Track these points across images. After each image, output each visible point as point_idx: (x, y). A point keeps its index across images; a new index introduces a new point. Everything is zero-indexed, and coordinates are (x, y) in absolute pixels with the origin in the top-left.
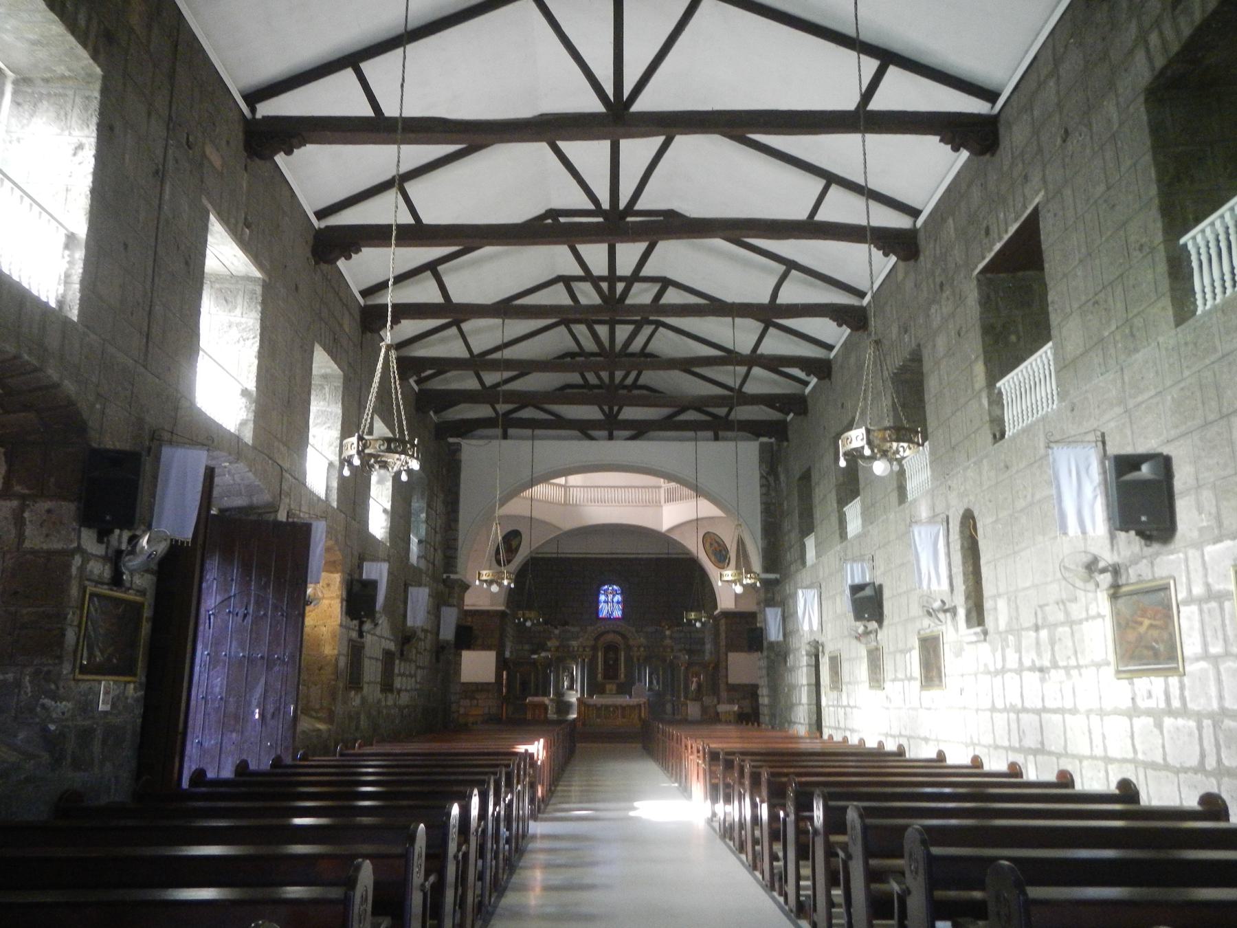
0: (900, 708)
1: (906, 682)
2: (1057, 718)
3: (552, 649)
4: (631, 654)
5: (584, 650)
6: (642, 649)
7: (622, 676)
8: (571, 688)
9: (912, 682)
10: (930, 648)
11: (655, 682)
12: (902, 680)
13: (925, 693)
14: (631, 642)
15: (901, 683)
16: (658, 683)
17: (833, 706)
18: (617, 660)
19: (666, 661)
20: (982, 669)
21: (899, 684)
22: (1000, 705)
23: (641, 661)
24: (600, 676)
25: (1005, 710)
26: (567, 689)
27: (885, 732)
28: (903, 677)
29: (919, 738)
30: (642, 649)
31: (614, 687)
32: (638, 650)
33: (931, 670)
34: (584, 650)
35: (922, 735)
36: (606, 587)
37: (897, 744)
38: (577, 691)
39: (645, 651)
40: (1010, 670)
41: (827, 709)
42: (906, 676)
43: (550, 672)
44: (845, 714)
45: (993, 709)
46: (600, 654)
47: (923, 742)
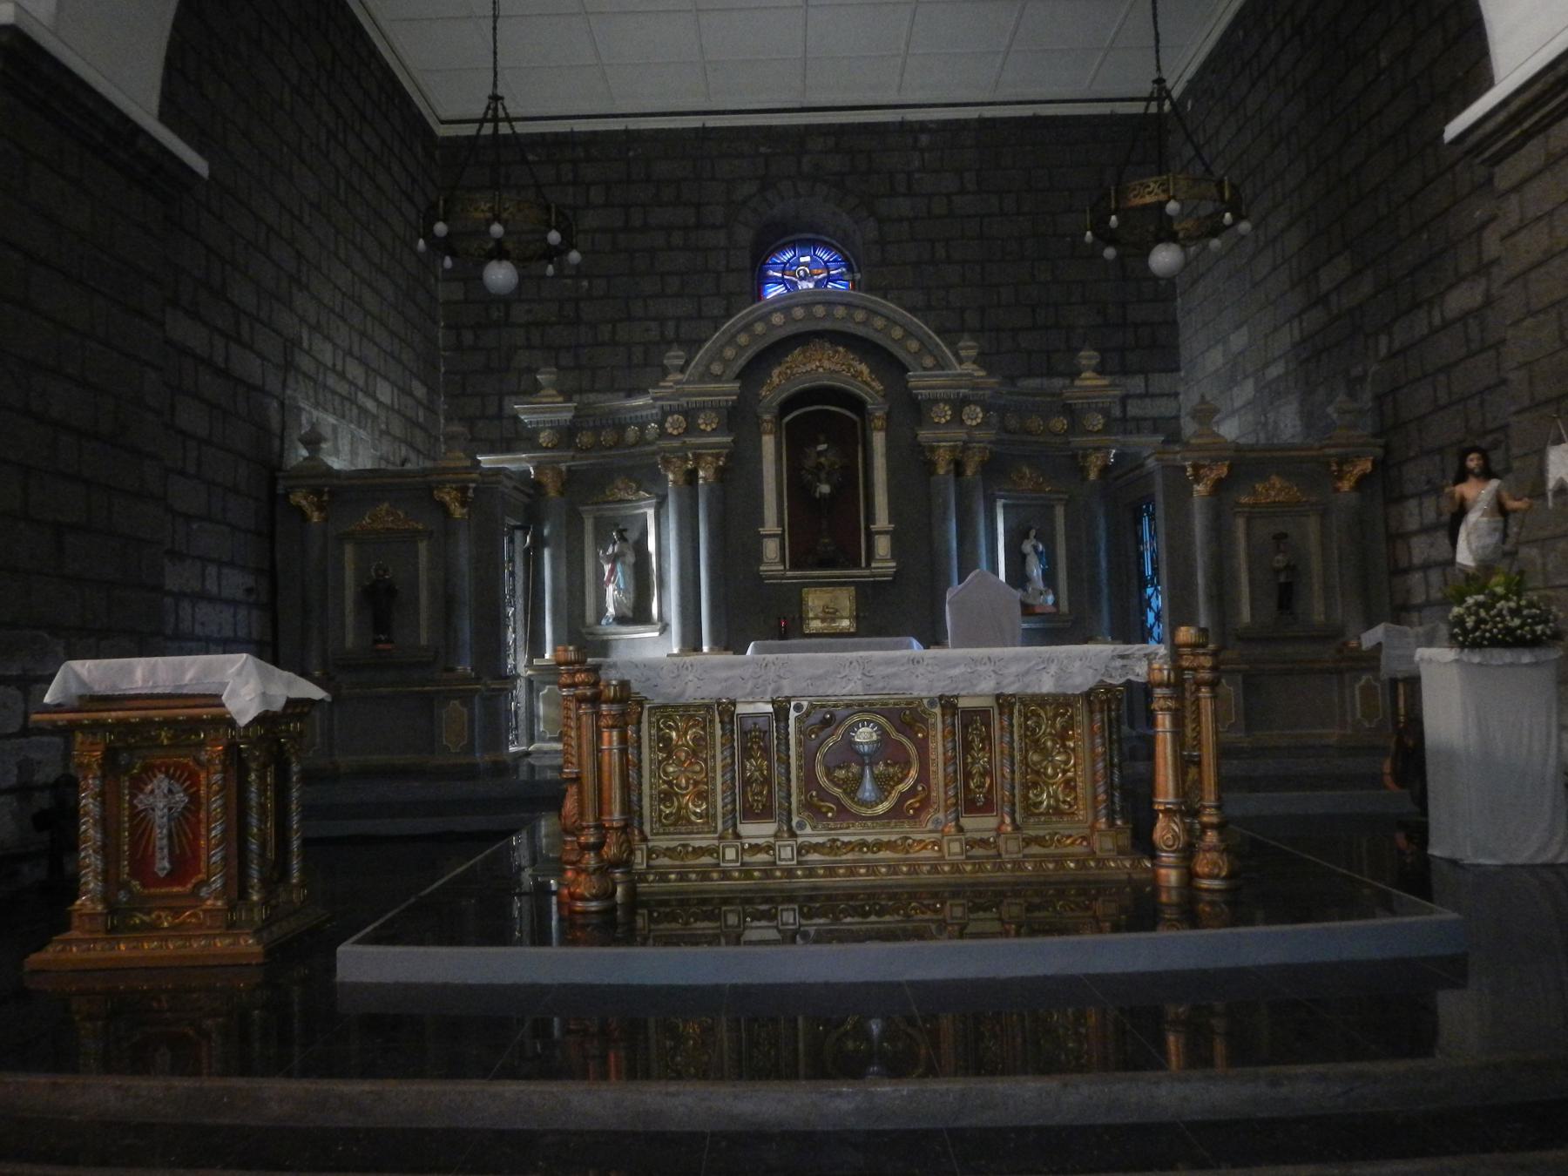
3: (544, 438)
4: (924, 435)
5: (692, 429)
6: (973, 415)
7: (883, 546)
8: (638, 614)
11: (1035, 570)
14: (921, 381)
16: (1049, 578)
18: (852, 484)
19: (1083, 471)
23: (969, 472)
24: (771, 549)
26: (621, 620)
30: (973, 415)
31: (845, 600)
32: (957, 419)
34: (692, 429)
36: (789, 255)
38: (665, 628)
39: (985, 424)
43: (539, 543)
46: (768, 443)
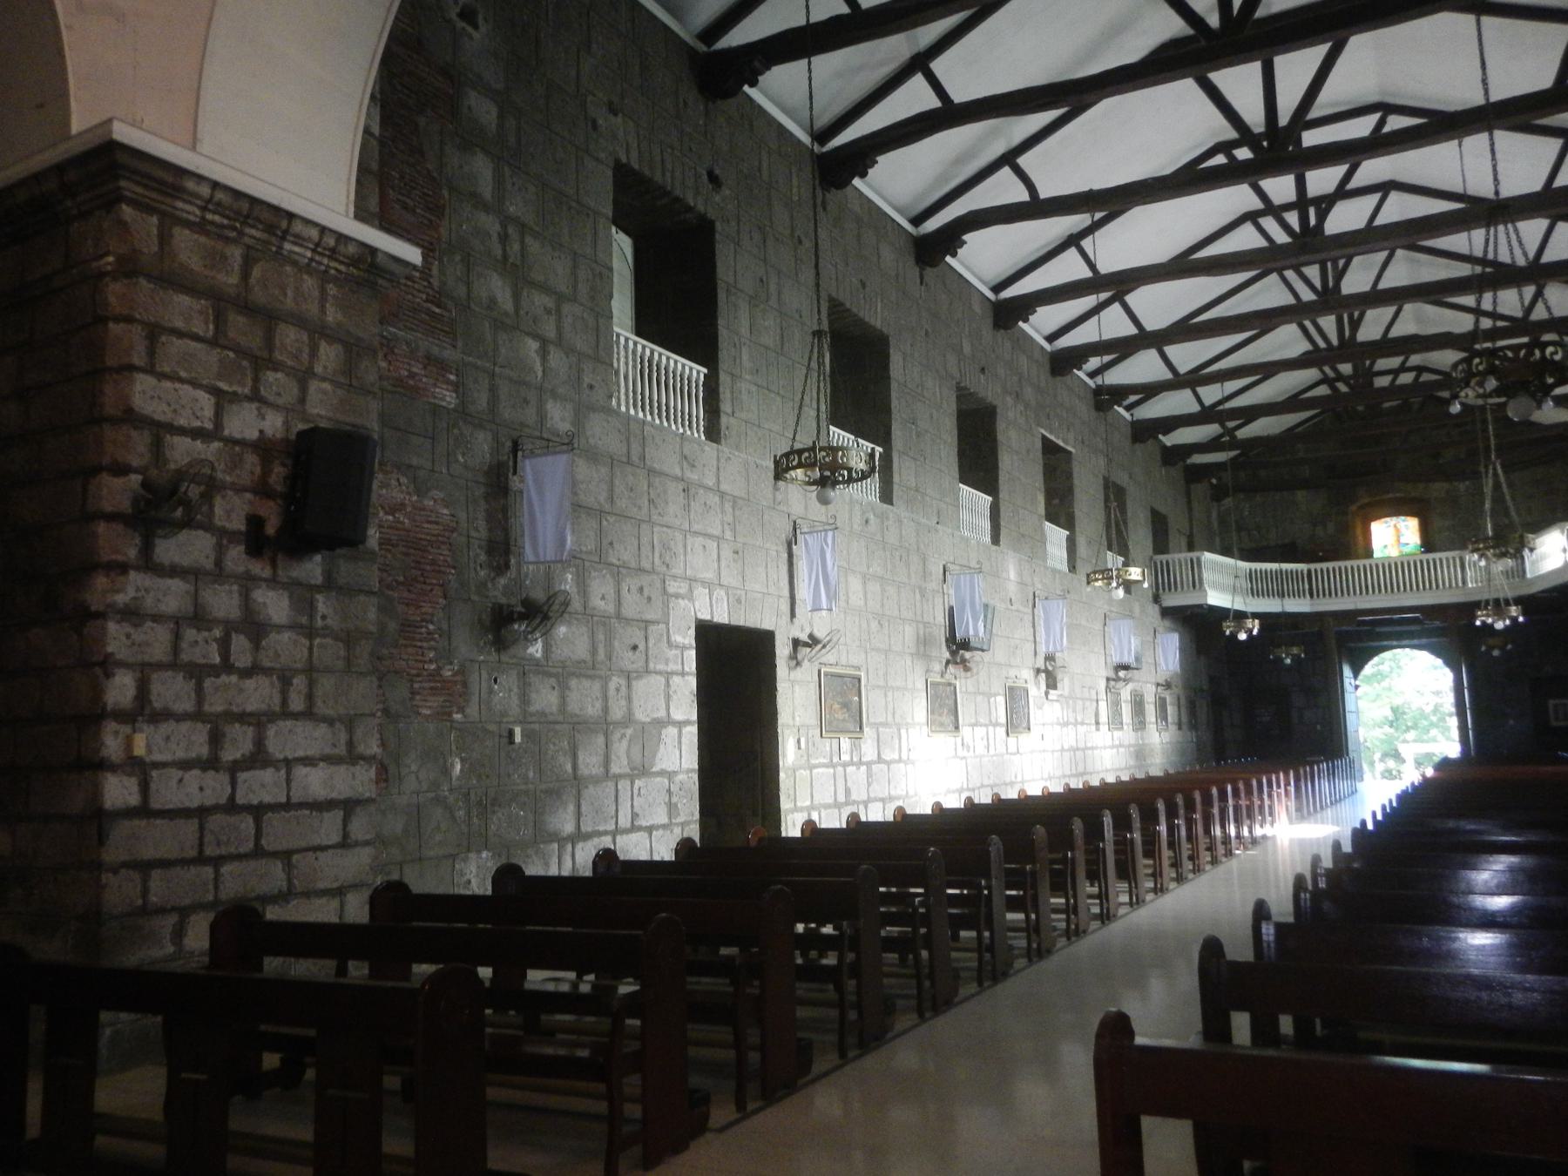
0: (981, 756)
1: (991, 728)
2: (1090, 752)
9: (998, 729)
10: (1015, 698)
12: (986, 725)
13: (1012, 740)
15: (984, 729)
17: (832, 765)
20: (1055, 721)
21: (980, 731)
22: (1066, 747)
25: (1069, 750)
27: (959, 786)
28: (987, 722)
29: (1006, 784)
33: (1016, 721)
35: (1008, 780)
37: (1063, 784)
40: (1071, 723)
41: (803, 774)
42: (991, 721)
44: (869, 775)
45: (1062, 750)
47: (1009, 787)
